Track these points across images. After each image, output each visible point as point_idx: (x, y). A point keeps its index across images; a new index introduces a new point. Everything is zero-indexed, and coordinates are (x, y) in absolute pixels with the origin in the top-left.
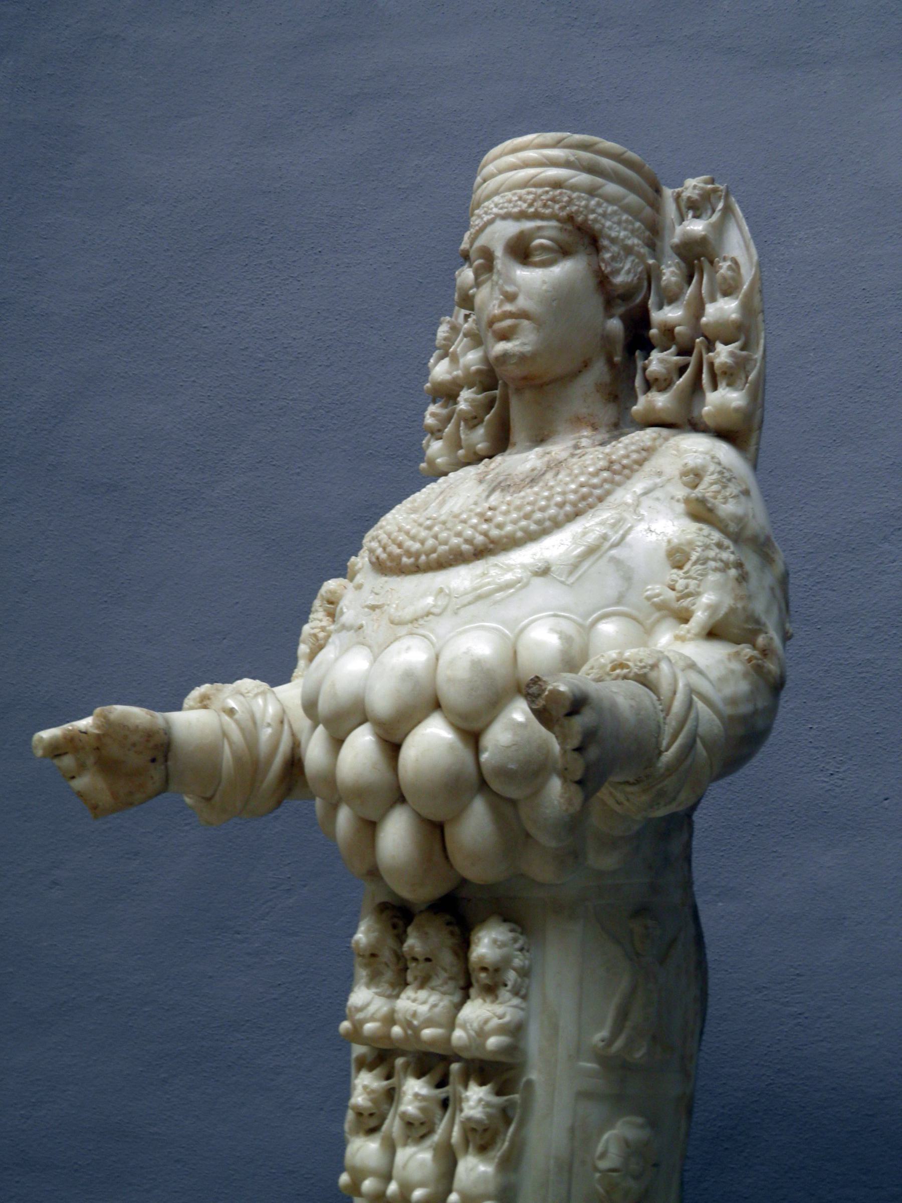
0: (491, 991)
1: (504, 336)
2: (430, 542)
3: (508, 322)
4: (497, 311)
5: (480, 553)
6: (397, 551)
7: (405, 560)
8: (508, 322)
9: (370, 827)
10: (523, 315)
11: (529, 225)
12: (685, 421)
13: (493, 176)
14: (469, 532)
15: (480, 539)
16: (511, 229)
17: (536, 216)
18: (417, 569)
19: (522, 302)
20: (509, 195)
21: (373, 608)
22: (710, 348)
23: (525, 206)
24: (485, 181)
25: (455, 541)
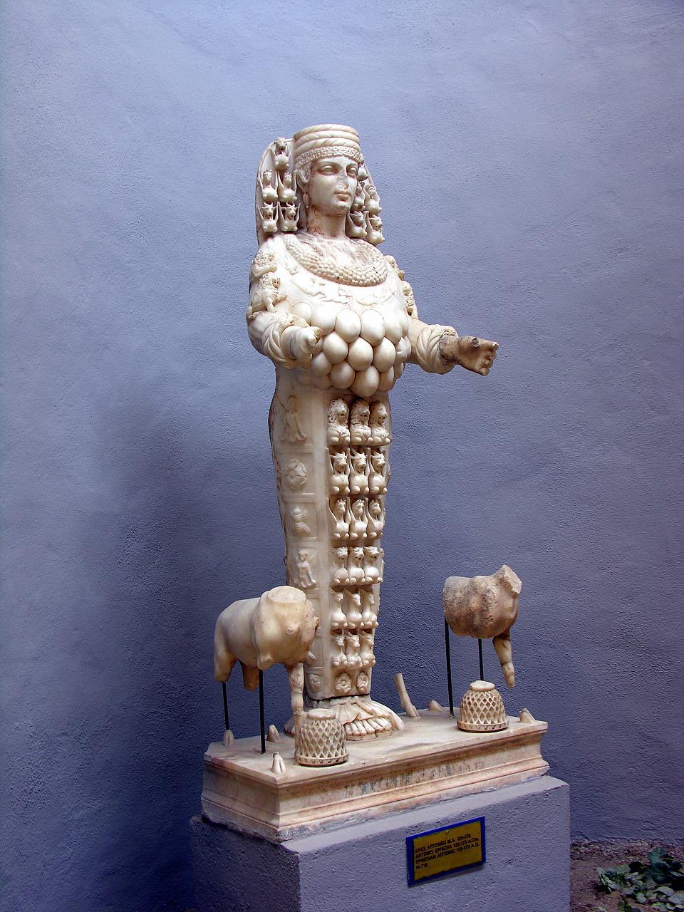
0: (380, 424)
1: (343, 200)
2: (364, 277)
3: (346, 196)
4: (343, 190)
5: (377, 283)
6: (350, 277)
7: (353, 280)
8: (346, 196)
9: (358, 372)
10: (350, 194)
11: (354, 162)
12: (367, 239)
13: (338, 137)
14: (374, 276)
15: (378, 279)
16: (347, 162)
17: (354, 160)
18: (358, 285)
19: (349, 190)
20: (348, 149)
21: (347, 297)
22: (370, 215)
23: (353, 155)
24: (332, 137)
25: (371, 278)
